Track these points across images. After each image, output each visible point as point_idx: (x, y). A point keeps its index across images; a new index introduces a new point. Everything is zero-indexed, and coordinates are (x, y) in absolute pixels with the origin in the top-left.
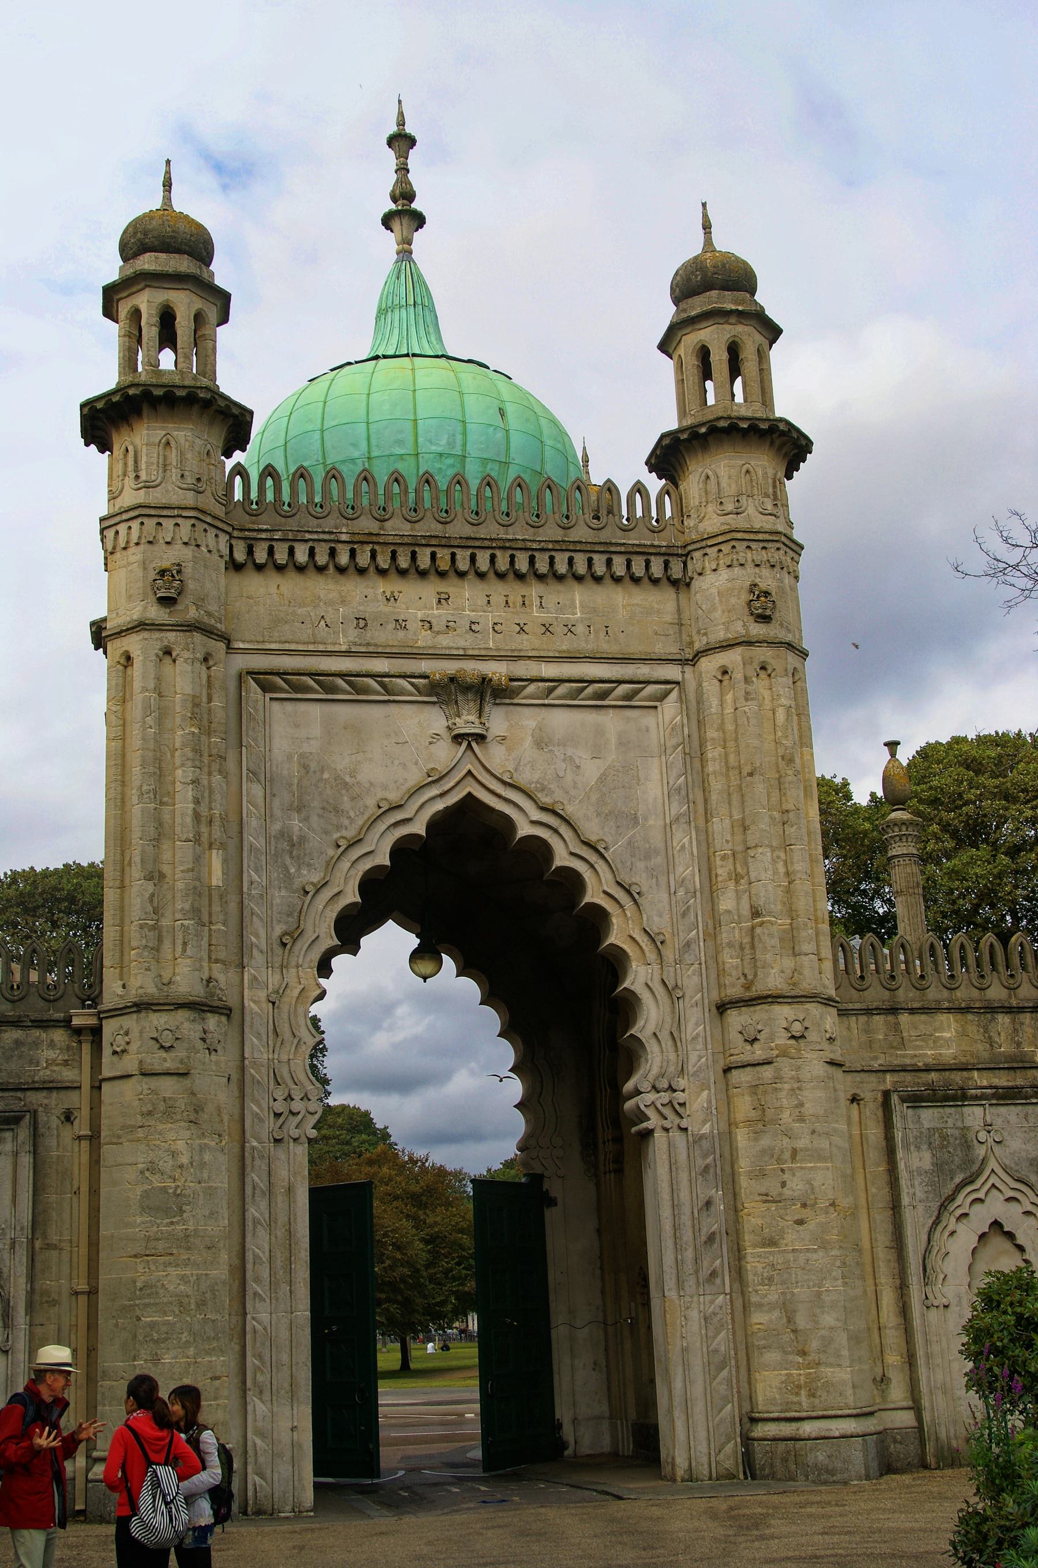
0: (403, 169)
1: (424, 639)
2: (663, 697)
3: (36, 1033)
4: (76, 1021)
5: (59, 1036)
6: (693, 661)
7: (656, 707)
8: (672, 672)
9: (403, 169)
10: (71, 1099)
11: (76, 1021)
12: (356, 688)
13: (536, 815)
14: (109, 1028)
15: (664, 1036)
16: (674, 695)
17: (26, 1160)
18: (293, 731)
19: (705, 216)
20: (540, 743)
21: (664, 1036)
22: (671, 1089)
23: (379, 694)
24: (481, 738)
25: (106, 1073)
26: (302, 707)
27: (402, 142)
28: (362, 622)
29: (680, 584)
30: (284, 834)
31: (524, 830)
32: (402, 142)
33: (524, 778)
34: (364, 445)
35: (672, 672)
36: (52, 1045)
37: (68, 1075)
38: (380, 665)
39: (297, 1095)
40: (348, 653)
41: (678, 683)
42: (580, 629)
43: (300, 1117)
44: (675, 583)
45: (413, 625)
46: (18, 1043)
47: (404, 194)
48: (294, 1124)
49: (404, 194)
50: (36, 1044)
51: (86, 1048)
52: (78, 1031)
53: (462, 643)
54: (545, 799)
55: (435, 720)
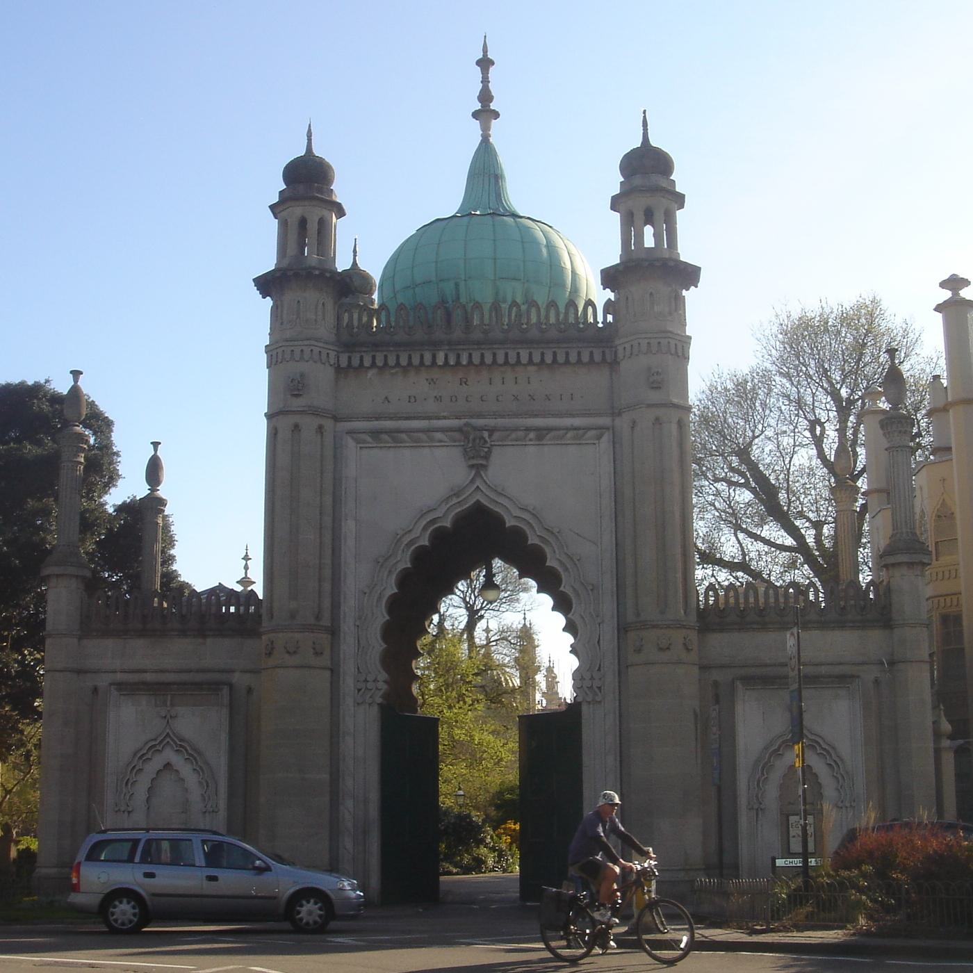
0: (485, 81)
2: (599, 437)
6: (620, 414)
7: (594, 444)
8: (605, 421)
9: (485, 81)
16: (605, 438)
19: (645, 117)
23: (426, 442)
27: (485, 63)
31: (510, 522)
32: (485, 63)
41: (608, 429)
43: (373, 691)
47: (485, 96)
48: (369, 696)
49: (485, 96)
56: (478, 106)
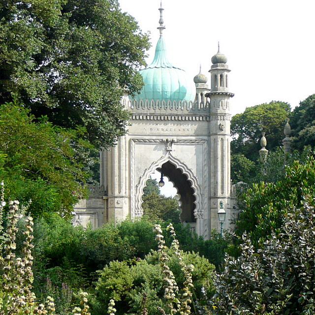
1: (162, 132)
3: (97, 199)
4: (104, 198)
5: (101, 200)
10: (103, 210)
11: (104, 198)
12: (150, 142)
13: (180, 164)
14: (109, 200)
15: (200, 202)
17: (97, 220)
18: (137, 149)
20: (182, 151)
21: (200, 202)
22: (201, 211)
24: (171, 151)
25: (109, 206)
26: (140, 145)
27: (161, 10)
28: (151, 129)
29: (209, 121)
30: (137, 167)
32: (161, 10)
33: (178, 158)
34: (152, 89)
35: (206, 138)
36: (100, 201)
37: (102, 206)
38: (154, 138)
39: (139, 211)
40: (149, 135)
42: (190, 130)
44: (208, 121)
45: (160, 130)
46: (95, 201)
49: (161, 23)
50: (97, 201)
51: (106, 202)
52: (104, 200)
53: (169, 133)
54: (182, 161)
55: (163, 147)
56: (159, 26)
